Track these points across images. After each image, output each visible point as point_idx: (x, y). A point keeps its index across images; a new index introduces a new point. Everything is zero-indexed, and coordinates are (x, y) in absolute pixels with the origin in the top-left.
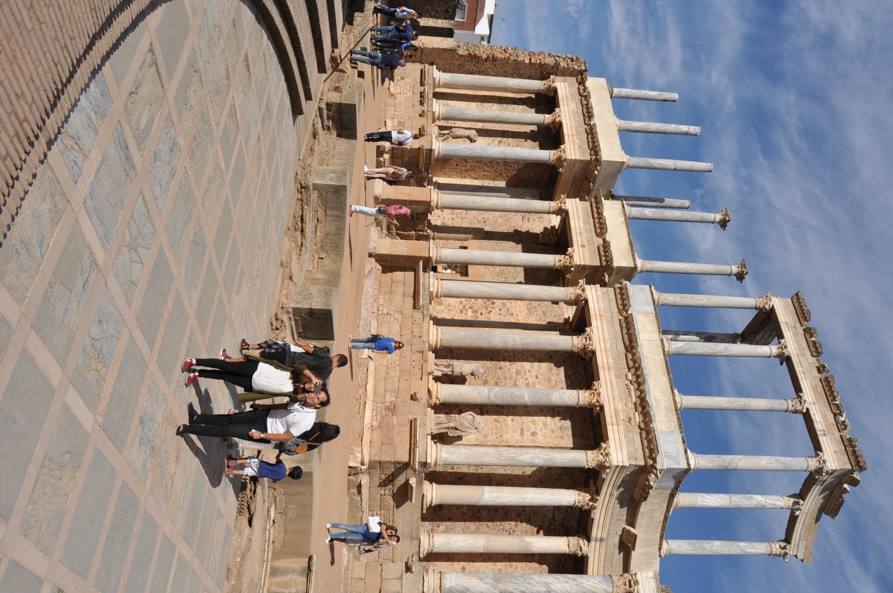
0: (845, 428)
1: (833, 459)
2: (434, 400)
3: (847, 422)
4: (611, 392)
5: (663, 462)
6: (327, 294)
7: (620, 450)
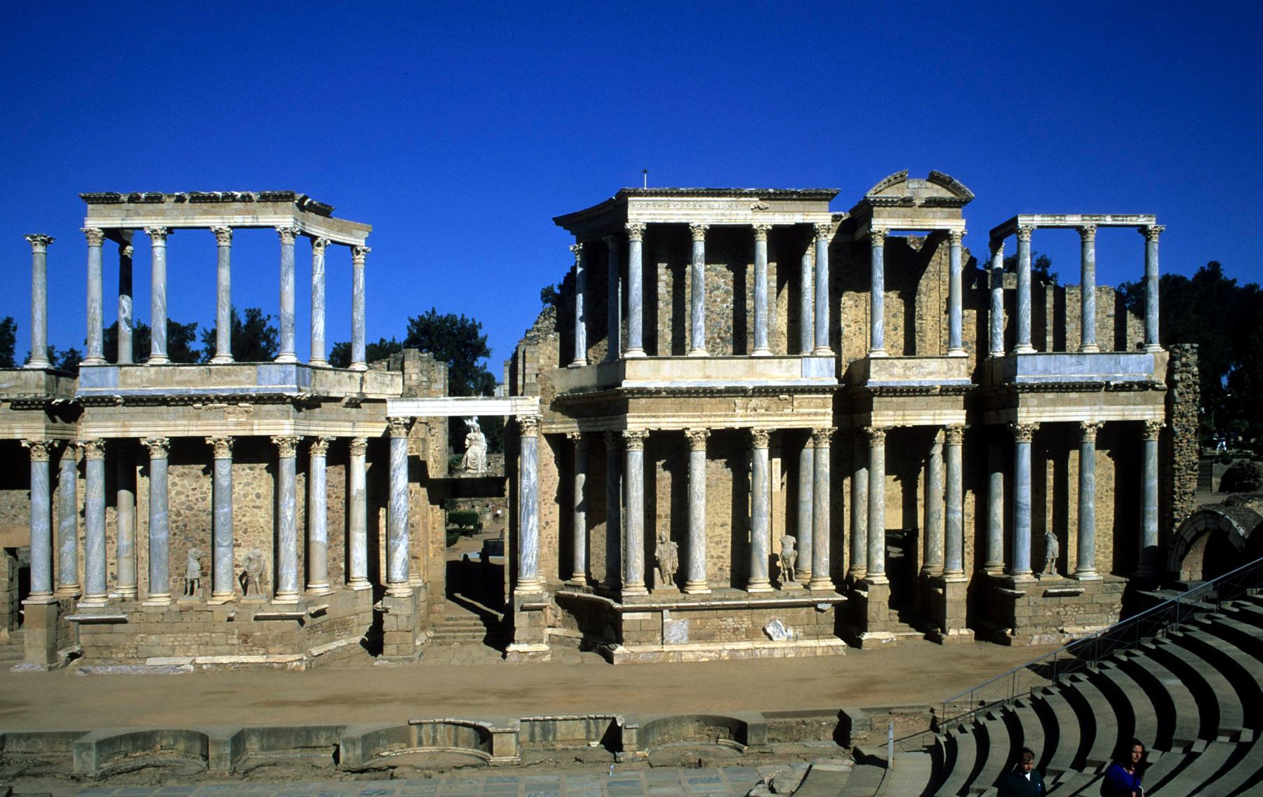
0: (250, 197)
1: (283, 219)
3: (245, 193)
4: (219, 428)
7: (281, 427)
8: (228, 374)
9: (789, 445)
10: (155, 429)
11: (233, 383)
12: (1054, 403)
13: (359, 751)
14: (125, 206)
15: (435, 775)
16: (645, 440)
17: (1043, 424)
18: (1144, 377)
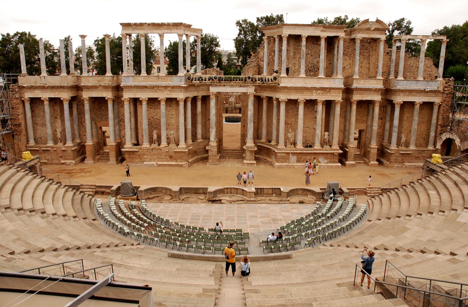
2: (167, 145)
4: (162, 95)
5: (183, 84)
6: (175, 192)
8: (164, 79)
9: (329, 105)
10: (144, 96)
11: (166, 81)
12: (408, 95)
13: (212, 196)
14: (132, 27)
15: (233, 203)
16: (286, 102)
17: (404, 102)
18: (436, 88)
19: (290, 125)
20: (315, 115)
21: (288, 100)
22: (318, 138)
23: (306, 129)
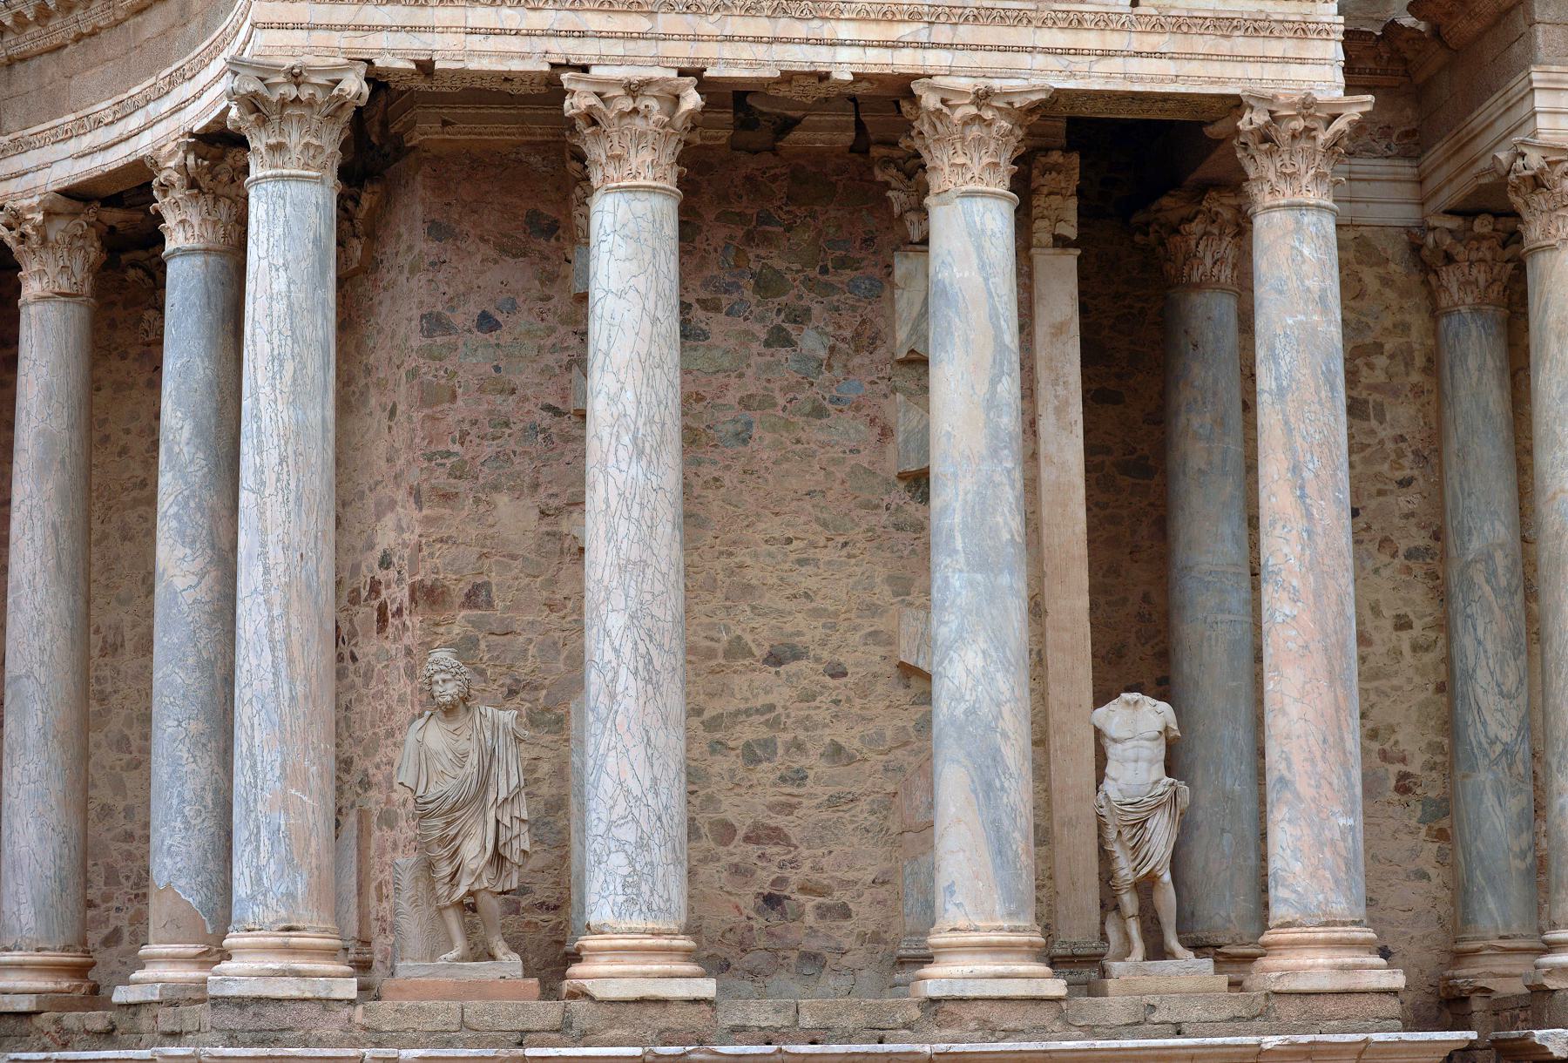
19: (460, 622)
20: (903, 418)
21: (377, 80)
22: (987, 791)
23: (755, 685)
